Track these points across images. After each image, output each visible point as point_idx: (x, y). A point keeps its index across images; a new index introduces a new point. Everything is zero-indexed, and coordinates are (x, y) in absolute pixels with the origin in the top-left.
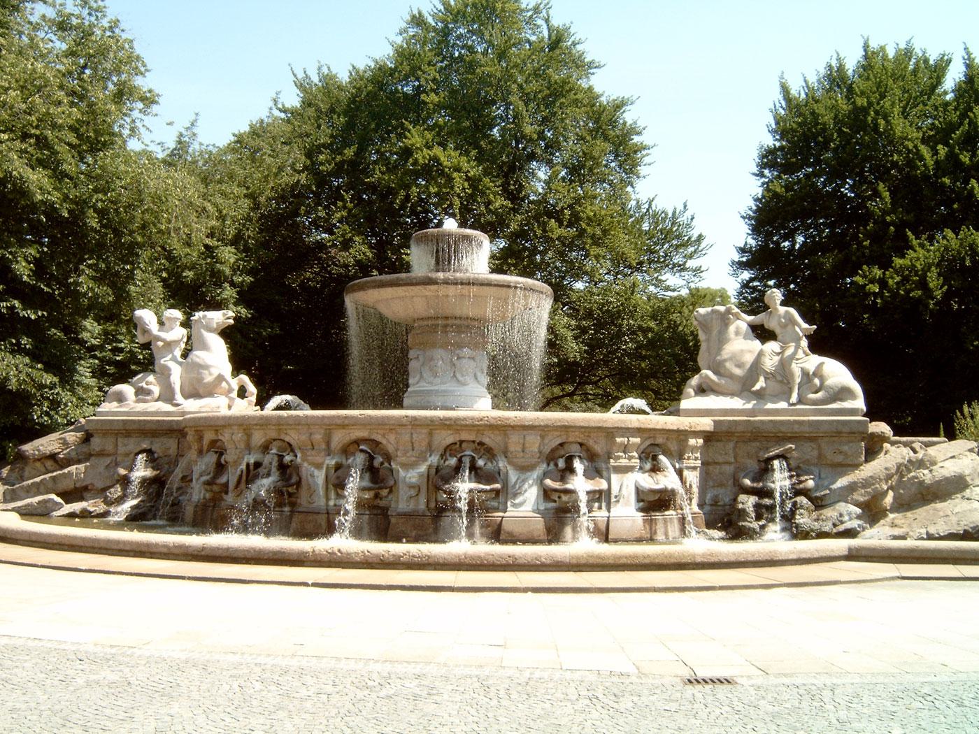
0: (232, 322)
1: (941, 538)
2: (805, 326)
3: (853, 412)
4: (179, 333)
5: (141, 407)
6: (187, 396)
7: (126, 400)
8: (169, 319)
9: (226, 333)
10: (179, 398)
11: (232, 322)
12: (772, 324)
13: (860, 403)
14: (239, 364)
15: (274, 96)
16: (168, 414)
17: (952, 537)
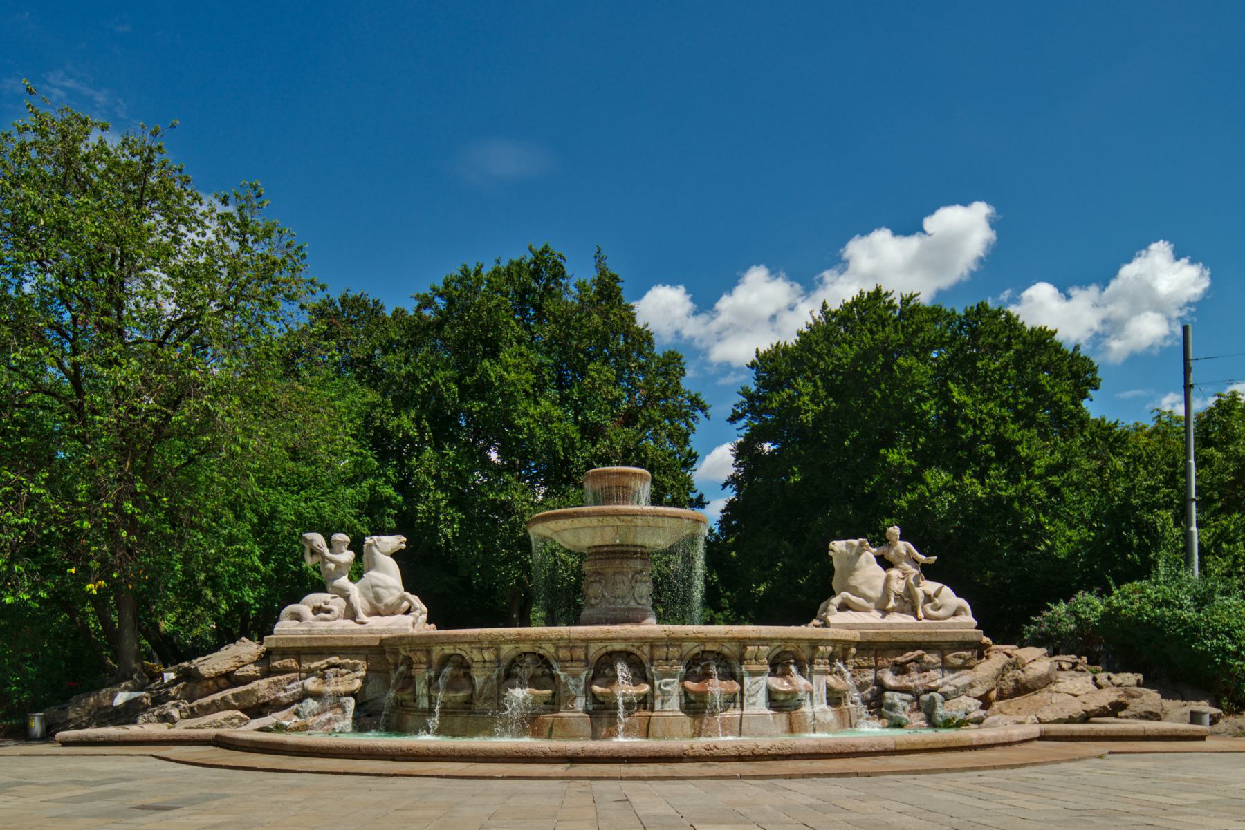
0: (404, 546)
1: (1051, 722)
2: (922, 558)
3: (962, 625)
4: (347, 556)
5: (323, 626)
6: (370, 615)
7: (306, 619)
8: (340, 543)
9: (396, 555)
10: (362, 617)
11: (404, 546)
12: (891, 555)
13: (968, 619)
14: (410, 583)
15: (709, 412)
16: (353, 632)
17: (1060, 721)
